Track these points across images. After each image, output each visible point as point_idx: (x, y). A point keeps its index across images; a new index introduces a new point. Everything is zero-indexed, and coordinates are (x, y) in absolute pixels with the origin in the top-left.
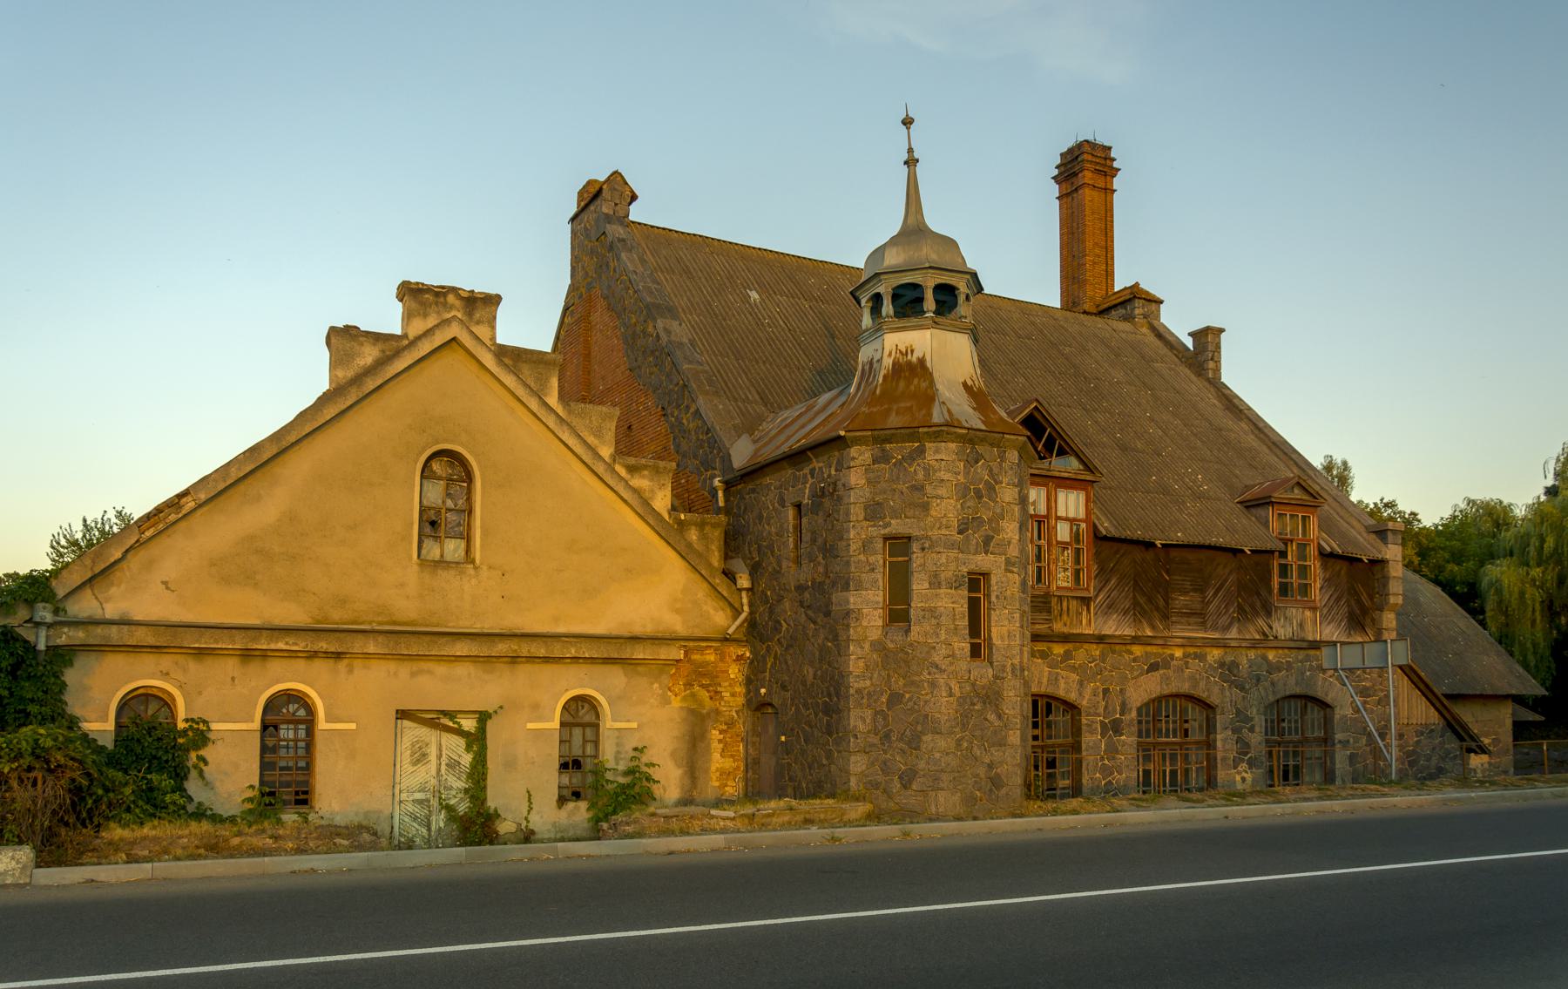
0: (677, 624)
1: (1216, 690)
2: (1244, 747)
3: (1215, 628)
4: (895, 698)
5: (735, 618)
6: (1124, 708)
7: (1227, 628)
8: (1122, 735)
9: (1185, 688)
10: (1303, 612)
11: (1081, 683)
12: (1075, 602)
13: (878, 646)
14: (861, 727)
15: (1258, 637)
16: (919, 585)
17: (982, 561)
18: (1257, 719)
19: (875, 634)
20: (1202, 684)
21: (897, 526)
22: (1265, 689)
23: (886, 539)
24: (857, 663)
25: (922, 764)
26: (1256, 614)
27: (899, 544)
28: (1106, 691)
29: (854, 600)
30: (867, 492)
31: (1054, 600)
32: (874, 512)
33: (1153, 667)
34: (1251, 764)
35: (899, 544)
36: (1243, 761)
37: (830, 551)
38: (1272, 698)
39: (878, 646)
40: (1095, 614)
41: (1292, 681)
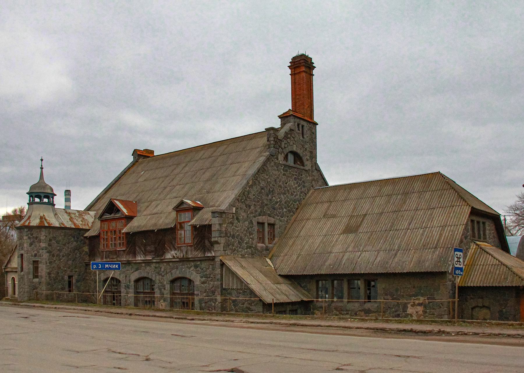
1: (154, 275)
2: (162, 294)
6: (130, 281)
8: (130, 289)
9: (145, 275)
10: (187, 247)
11: (120, 274)
12: (122, 252)
15: (171, 257)
18: (166, 285)
20: (150, 274)
22: (169, 275)
26: (171, 250)
28: (126, 276)
31: (117, 252)
33: (137, 270)
34: (164, 301)
36: (162, 299)
38: (171, 278)
40: (127, 254)
41: (178, 272)
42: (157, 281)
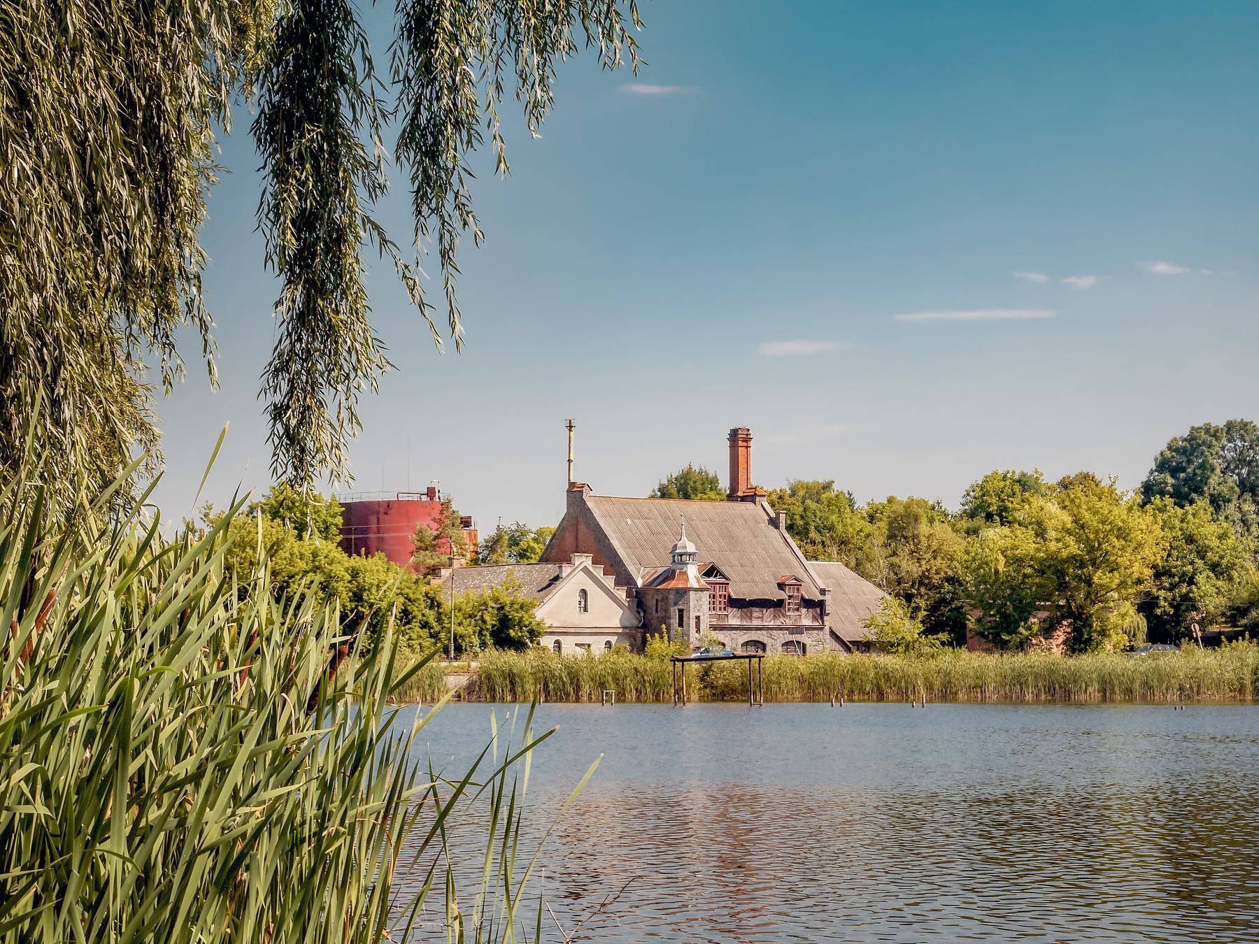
16: (685, 619)
17: (698, 614)
21: (681, 607)
27: (681, 611)
35: (681, 611)
42: (770, 645)
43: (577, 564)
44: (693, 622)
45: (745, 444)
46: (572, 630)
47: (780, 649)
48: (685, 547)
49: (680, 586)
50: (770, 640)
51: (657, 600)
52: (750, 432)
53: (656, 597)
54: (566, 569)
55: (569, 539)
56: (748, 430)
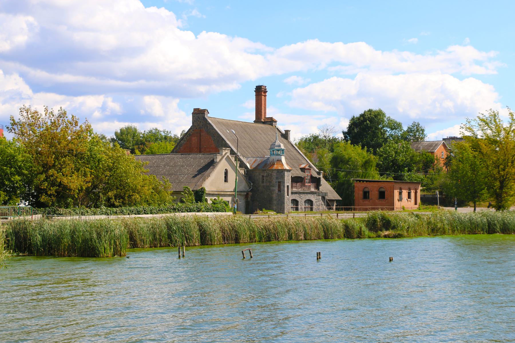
0: (244, 190)
3: (298, 189)
4: (279, 200)
5: (249, 189)
7: (299, 189)
13: (277, 194)
14: (275, 203)
16: (282, 187)
19: (277, 192)
21: (280, 180)
23: (278, 182)
24: (274, 196)
25: (282, 207)
27: (279, 182)
29: (274, 188)
30: (276, 176)
32: (277, 178)
35: (279, 182)
37: (270, 182)
39: (277, 194)
43: (224, 153)
44: (286, 189)
45: (264, 94)
46: (222, 193)
47: (304, 204)
48: (280, 146)
49: (280, 168)
50: (300, 199)
51: (263, 176)
52: (266, 88)
53: (262, 174)
54: (219, 157)
55: (195, 139)
56: (266, 87)
